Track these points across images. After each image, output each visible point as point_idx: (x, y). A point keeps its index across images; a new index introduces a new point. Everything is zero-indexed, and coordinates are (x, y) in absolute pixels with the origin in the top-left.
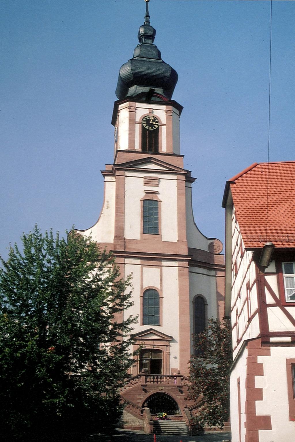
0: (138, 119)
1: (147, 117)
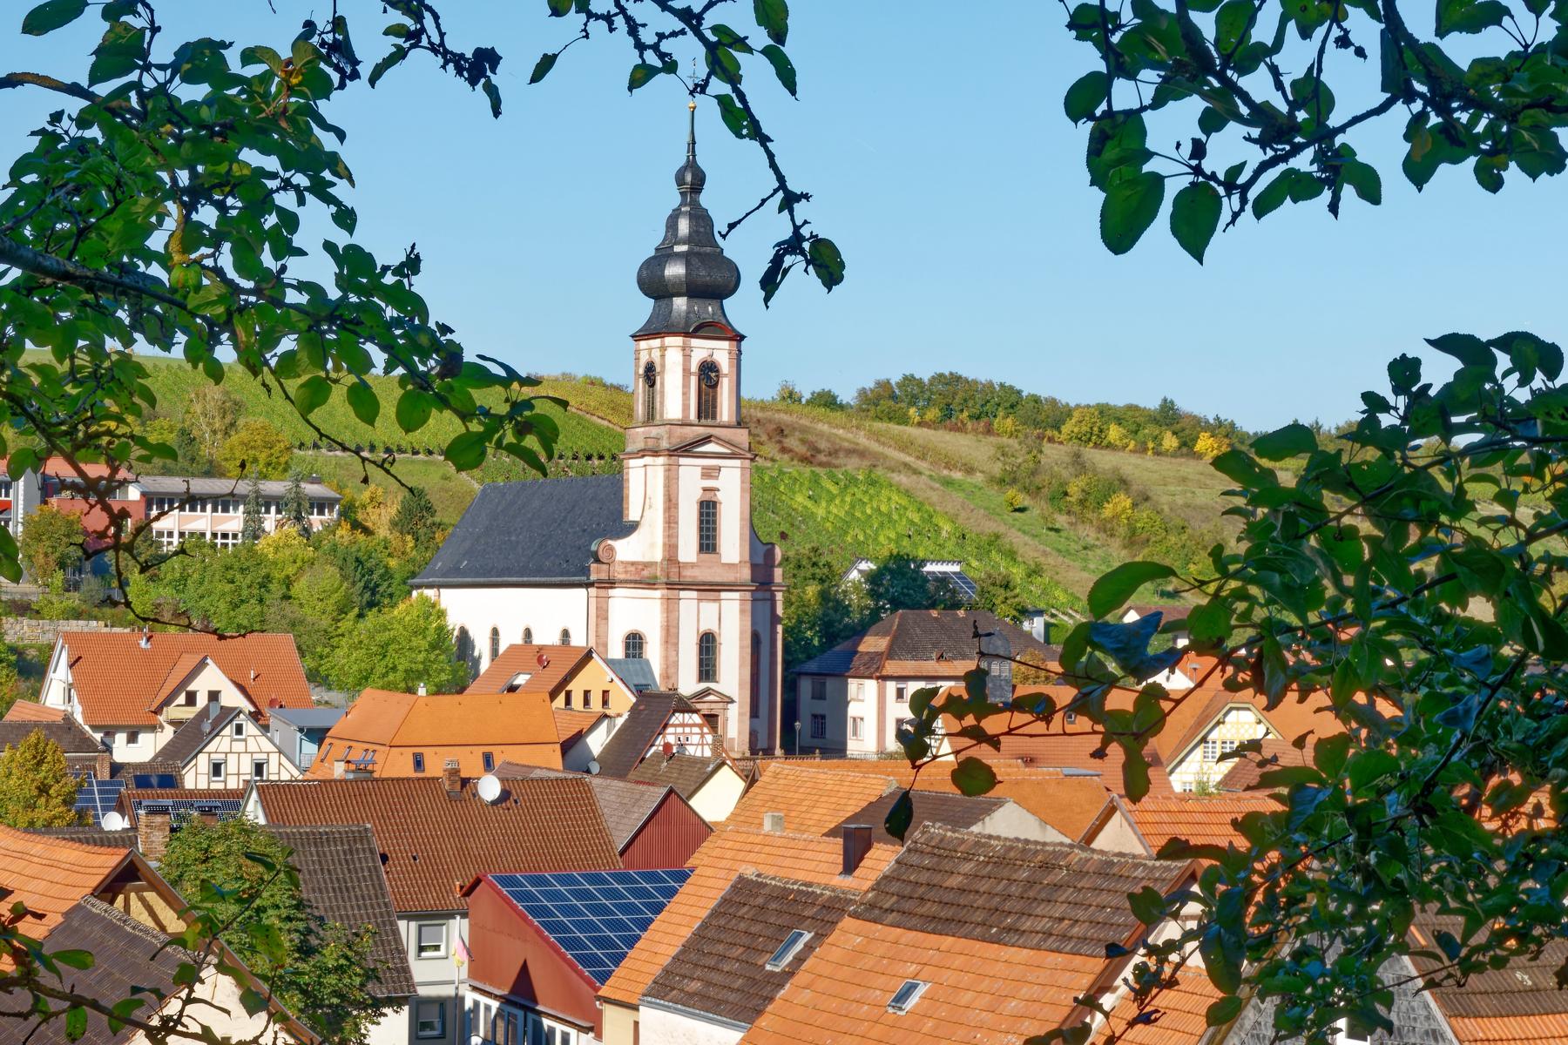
0: (694, 368)
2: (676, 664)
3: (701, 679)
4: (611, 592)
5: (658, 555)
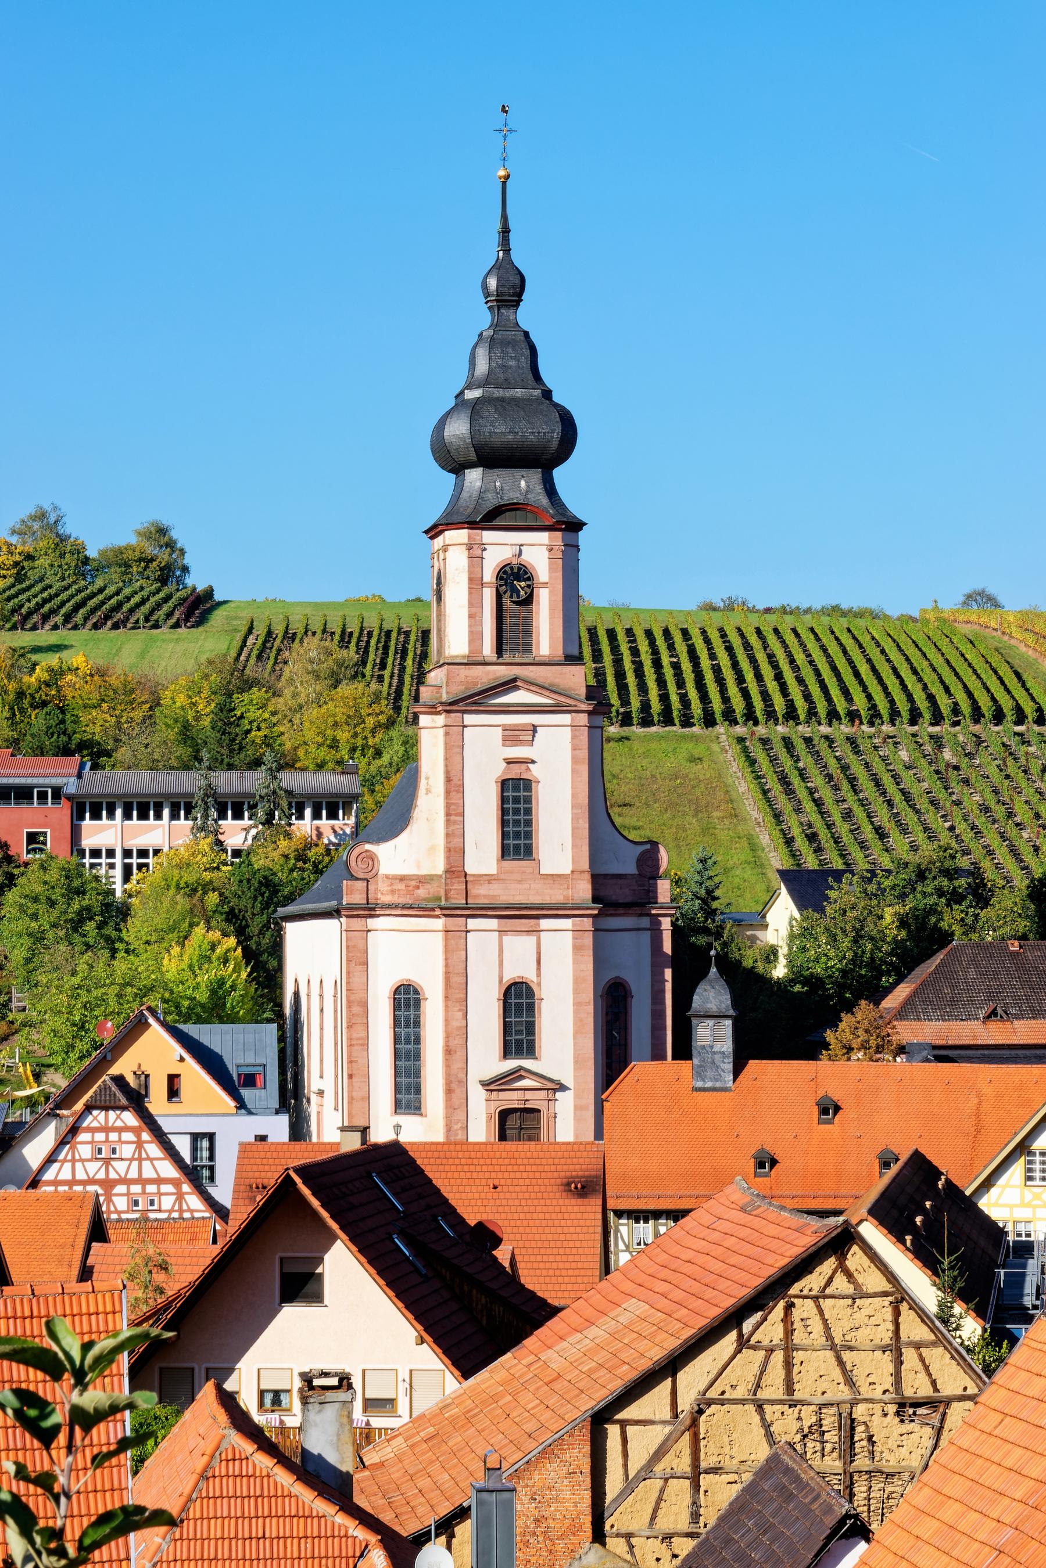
0: (489, 575)
1: (507, 569)
3: (507, 1052)
4: (372, 923)
5: (439, 866)
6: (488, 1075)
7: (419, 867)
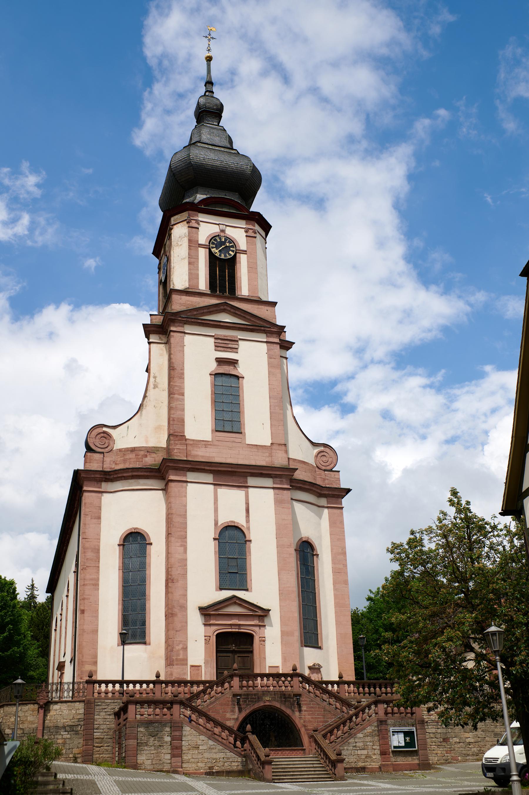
2: (184, 563)
6: (206, 602)
7: (147, 441)
